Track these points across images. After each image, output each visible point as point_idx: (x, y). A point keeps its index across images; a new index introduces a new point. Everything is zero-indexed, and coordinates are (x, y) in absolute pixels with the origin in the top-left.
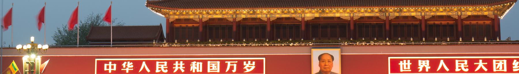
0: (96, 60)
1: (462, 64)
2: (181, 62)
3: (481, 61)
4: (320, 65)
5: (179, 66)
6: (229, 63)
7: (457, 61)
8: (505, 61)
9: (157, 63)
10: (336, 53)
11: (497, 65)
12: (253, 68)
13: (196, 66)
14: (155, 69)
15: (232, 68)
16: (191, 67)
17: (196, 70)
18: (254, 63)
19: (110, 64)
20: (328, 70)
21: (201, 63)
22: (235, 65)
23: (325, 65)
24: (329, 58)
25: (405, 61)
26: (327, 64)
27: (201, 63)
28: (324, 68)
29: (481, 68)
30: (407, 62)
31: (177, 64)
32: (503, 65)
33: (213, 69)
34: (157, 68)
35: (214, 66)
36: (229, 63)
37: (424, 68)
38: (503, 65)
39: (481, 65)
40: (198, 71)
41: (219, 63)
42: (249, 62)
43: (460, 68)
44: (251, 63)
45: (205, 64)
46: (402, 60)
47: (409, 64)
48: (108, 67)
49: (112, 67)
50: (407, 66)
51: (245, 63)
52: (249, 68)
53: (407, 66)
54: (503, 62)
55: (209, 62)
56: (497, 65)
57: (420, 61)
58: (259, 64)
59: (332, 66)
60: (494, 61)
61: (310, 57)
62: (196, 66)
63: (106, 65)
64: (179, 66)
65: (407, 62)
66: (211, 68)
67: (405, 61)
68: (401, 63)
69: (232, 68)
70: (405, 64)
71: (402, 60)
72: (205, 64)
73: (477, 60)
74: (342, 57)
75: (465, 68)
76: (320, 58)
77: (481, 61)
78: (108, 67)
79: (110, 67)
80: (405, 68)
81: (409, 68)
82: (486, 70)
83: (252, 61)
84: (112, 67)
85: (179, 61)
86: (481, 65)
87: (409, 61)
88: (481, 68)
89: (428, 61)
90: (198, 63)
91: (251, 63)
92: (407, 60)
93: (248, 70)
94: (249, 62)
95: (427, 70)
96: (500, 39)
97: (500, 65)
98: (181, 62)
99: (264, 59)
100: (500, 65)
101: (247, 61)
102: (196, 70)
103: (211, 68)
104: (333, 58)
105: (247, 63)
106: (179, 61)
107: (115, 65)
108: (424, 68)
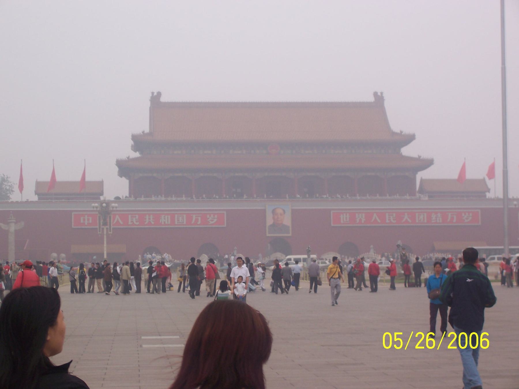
0: (73, 213)
2: (151, 216)
3: (406, 214)
4: (273, 218)
5: (149, 219)
8: (425, 214)
12: (215, 220)
13: (165, 219)
15: (197, 220)
16: (161, 220)
17: (165, 222)
18: (216, 216)
19: (86, 217)
21: (169, 217)
22: (200, 218)
25: (345, 214)
29: (406, 220)
30: (346, 215)
31: (147, 217)
33: (180, 221)
35: (180, 219)
37: (360, 220)
39: (406, 217)
40: (166, 223)
41: (185, 216)
42: (212, 216)
43: (389, 220)
48: (84, 220)
49: (88, 220)
50: (346, 218)
51: (208, 216)
52: (212, 221)
53: (346, 218)
54: (424, 215)
55: (176, 215)
56: (419, 217)
57: (357, 215)
61: (264, 211)
62: (165, 219)
63: (82, 218)
64: (149, 219)
65: (346, 215)
66: (178, 220)
67: (345, 214)
68: (342, 216)
69: (197, 220)
74: (294, 212)
76: (274, 212)
77: (406, 214)
78: (84, 220)
79: (86, 220)
80: (345, 220)
81: (348, 220)
82: (410, 221)
84: (88, 220)
85: (149, 215)
86: (406, 217)
87: (348, 215)
88: (406, 220)
89: (364, 215)
90: (166, 217)
93: (211, 222)
94: (212, 216)
95: (363, 222)
97: (422, 217)
98: (151, 216)
99: (225, 212)
100: (422, 217)
102: (165, 222)
103: (178, 220)
104: (284, 211)
105: (210, 216)
106: (149, 215)
107: (91, 218)
108: (360, 220)
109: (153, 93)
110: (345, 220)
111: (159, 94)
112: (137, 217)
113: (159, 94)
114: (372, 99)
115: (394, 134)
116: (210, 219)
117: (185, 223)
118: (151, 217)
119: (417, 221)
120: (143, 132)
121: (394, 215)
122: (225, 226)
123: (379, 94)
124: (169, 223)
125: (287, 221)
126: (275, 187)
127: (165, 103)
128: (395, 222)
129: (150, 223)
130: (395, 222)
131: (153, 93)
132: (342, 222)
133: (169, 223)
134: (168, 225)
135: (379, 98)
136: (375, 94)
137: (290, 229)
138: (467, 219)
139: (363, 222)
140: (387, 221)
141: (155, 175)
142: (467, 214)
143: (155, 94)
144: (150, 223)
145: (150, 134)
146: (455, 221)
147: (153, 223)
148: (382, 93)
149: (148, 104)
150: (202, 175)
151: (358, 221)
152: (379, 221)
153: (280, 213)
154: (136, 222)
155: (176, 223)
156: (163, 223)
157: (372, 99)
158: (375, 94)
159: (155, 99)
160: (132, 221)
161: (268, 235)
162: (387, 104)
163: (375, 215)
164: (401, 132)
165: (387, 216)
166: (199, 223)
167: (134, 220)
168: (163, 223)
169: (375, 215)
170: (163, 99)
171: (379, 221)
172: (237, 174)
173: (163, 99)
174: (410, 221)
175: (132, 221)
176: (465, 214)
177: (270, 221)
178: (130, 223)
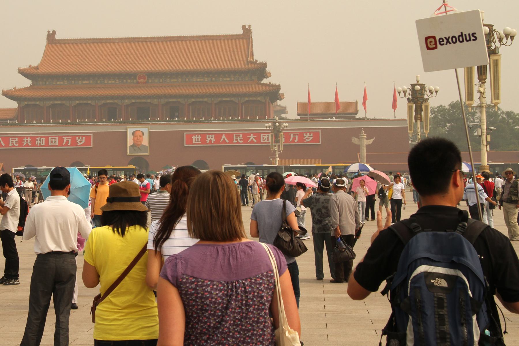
1: (239, 137)
3: (252, 135)
4: (133, 139)
5: (27, 141)
6: (65, 138)
7: (235, 135)
9: (11, 139)
10: (145, 130)
11: (263, 138)
12: (83, 141)
14: (9, 144)
15: (67, 142)
17: (40, 144)
18: (84, 138)
20: (139, 143)
21: (44, 139)
22: (70, 140)
23: (138, 139)
24: (141, 134)
26: (139, 138)
27: (44, 139)
28: (138, 142)
31: (25, 139)
32: (268, 138)
34: (11, 142)
35: (53, 141)
36: (65, 138)
37: (211, 140)
38: (268, 138)
39: (252, 137)
40: (41, 144)
41: (57, 138)
43: (236, 140)
44: (82, 138)
45: (47, 139)
46: (195, 135)
47: (199, 137)
50: (198, 139)
53: (198, 139)
55: (50, 138)
56: (263, 138)
57: (207, 135)
58: (88, 138)
59: (142, 140)
60: (262, 135)
61: (125, 134)
64: (27, 141)
66: (52, 142)
68: (194, 137)
69: (67, 142)
70: (196, 138)
71: (195, 135)
72: (47, 139)
73: (250, 134)
74: (151, 133)
75: (241, 140)
76: (134, 133)
77: (252, 135)
80: (197, 141)
81: (199, 140)
82: (255, 141)
83: (83, 136)
85: (27, 137)
86: (252, 137)
87: (199, 136)
89: (213, 135)
91: (82, 138)
92: (198, 134)
93: (80, 144)
95: (213, 142)
96: (269, 117)
97: (266, 137)
99: (92, 135)
100: (266, 137)
101: (79, 136)
102: (40, 144)
103: (52, 142)
104: (143, 133)
106: (27, 137)
108: (211, 140)
109: (49, 32)
110: (197, 141)
111: (54, 32)
112: (17, 140)
113: (54, 32)
114: (240, 32)
115: (251, 62)
116: (79, 140)
117: (57, 144)
118: (29, 139)
119: (262, 141)
120: (30, 66)
121: (241, 135)
122: (92, 147)
123: (247, 27)
124: (44, 144)
125: (145, 142)
126: (142, 113)
127: (59, 40)
128: (242, 142)
129: (27, 145)
130: (242, 142)
131: (49, 32)
132: (194, 142)
133: (44, 144)
134: (43, 146)
135: (247, 32)
136: (244, 27)
137: (149, 148)
138: (308, 139)
139: (213, 142)
140: (235, 141)
141: (38, 103)
142: (308, 134)
143: (51, 32)
144: (27, 145)
145: (37, 68)
146: (296, 141)
147: (30, 144)
148: (249, 26)
149: (45, 41)
150: (78, 102)
151: (208, 142)
152: (227, 141)
153: (139, 135)
154: (16, 143)
155: (50, 144)
156: (38, 145)
157: (240, 32)
158: (244, 27)
159: (51, 37)
160: (12, 143)
161: (129, 154)
162: (254, 36)
163: (224, 135)
164: (256, 61)
165: (235, 137)
166: (69, 144)
167: (14, 142)
168: (38, 145)
169: (224, 135)
170: (57, 37)
171: (227, 141)
172: (108, 101)
173: (57, 37)
174: (255, 141)
175: (12, 143)
176: (306, 134)
177: (130, 142)
178: (11, 145)
